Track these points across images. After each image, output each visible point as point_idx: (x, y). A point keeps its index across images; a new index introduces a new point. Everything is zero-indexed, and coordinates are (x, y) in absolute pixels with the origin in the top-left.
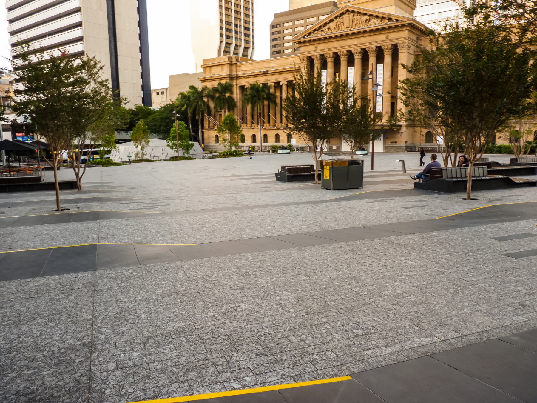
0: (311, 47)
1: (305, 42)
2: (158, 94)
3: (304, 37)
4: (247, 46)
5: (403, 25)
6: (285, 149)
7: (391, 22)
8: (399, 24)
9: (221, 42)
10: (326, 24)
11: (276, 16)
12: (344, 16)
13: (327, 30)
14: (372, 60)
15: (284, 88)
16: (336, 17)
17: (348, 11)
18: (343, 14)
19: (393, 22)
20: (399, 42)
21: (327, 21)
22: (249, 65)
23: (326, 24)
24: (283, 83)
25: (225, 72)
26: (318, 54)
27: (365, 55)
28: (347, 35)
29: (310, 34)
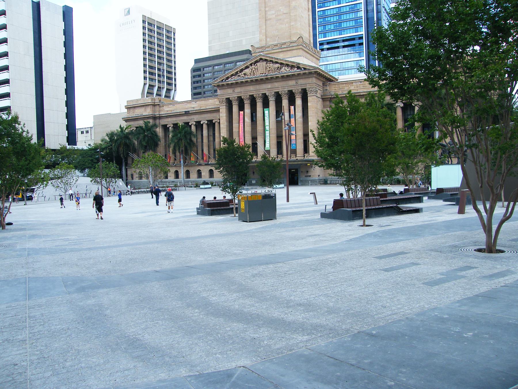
0: (229, 89)
1: (223, 85)
2: (82, 133)
3: (222, 81)
4: (169, 87)
5: (310, 73)
6: (207, 184)
9: (145, 84)
10: (242, 71)
11: (197, 61)
12: (258, 64)
14: (285, 103)
15: (205, 127)
16: (251, 65)
17: (261, 59)
18: (256, 62)
19: (301, 69)
20: (307, 87)
22: (171, 106)
23: (242, 71)
24: (204, 122)
25: (148, 112)
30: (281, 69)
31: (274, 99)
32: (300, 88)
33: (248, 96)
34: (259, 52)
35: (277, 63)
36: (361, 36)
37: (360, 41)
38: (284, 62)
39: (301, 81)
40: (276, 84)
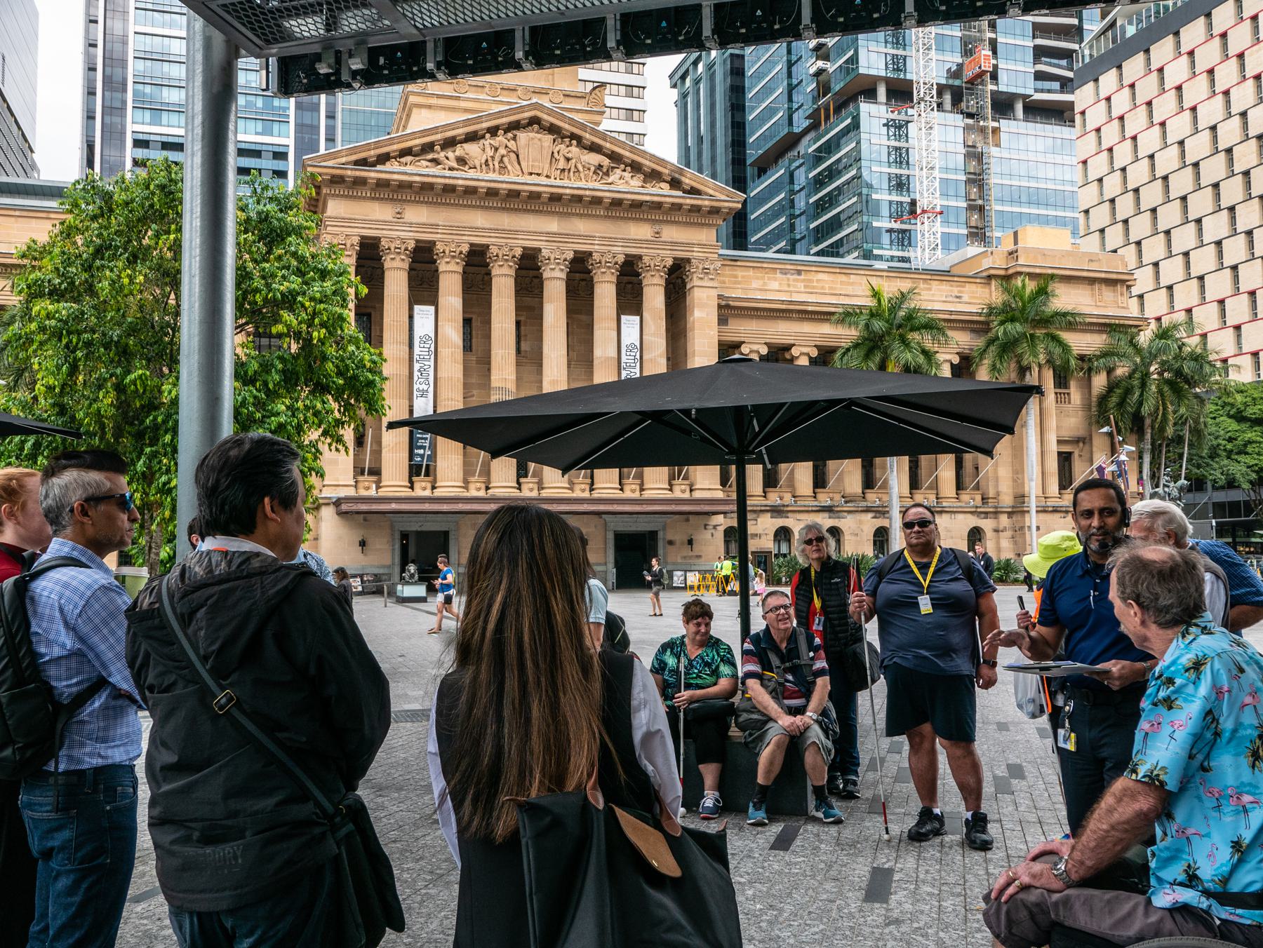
1: (360, 182)
7: (680, 193)
8: (706, 203)
10: (450, 143)
12: (523, 136)
13: (456, 165)
14: (605, 294)
16: (493, 131)
17: (534, 121)
18: (514, 126)
20: (696, 254)
21: (460, 132)
23: (450, 143)
26: (410, 237)
28: (534, 196)
29: (384, 158)
30: (607, 174)
31: (564, 276)
33: (465, 248)
34: (439, 96)
35: (594, 148)
36: (281, 150)
37: (278, 165)
38: (627, 154)
39: (671, 233)
40: (581, 226)
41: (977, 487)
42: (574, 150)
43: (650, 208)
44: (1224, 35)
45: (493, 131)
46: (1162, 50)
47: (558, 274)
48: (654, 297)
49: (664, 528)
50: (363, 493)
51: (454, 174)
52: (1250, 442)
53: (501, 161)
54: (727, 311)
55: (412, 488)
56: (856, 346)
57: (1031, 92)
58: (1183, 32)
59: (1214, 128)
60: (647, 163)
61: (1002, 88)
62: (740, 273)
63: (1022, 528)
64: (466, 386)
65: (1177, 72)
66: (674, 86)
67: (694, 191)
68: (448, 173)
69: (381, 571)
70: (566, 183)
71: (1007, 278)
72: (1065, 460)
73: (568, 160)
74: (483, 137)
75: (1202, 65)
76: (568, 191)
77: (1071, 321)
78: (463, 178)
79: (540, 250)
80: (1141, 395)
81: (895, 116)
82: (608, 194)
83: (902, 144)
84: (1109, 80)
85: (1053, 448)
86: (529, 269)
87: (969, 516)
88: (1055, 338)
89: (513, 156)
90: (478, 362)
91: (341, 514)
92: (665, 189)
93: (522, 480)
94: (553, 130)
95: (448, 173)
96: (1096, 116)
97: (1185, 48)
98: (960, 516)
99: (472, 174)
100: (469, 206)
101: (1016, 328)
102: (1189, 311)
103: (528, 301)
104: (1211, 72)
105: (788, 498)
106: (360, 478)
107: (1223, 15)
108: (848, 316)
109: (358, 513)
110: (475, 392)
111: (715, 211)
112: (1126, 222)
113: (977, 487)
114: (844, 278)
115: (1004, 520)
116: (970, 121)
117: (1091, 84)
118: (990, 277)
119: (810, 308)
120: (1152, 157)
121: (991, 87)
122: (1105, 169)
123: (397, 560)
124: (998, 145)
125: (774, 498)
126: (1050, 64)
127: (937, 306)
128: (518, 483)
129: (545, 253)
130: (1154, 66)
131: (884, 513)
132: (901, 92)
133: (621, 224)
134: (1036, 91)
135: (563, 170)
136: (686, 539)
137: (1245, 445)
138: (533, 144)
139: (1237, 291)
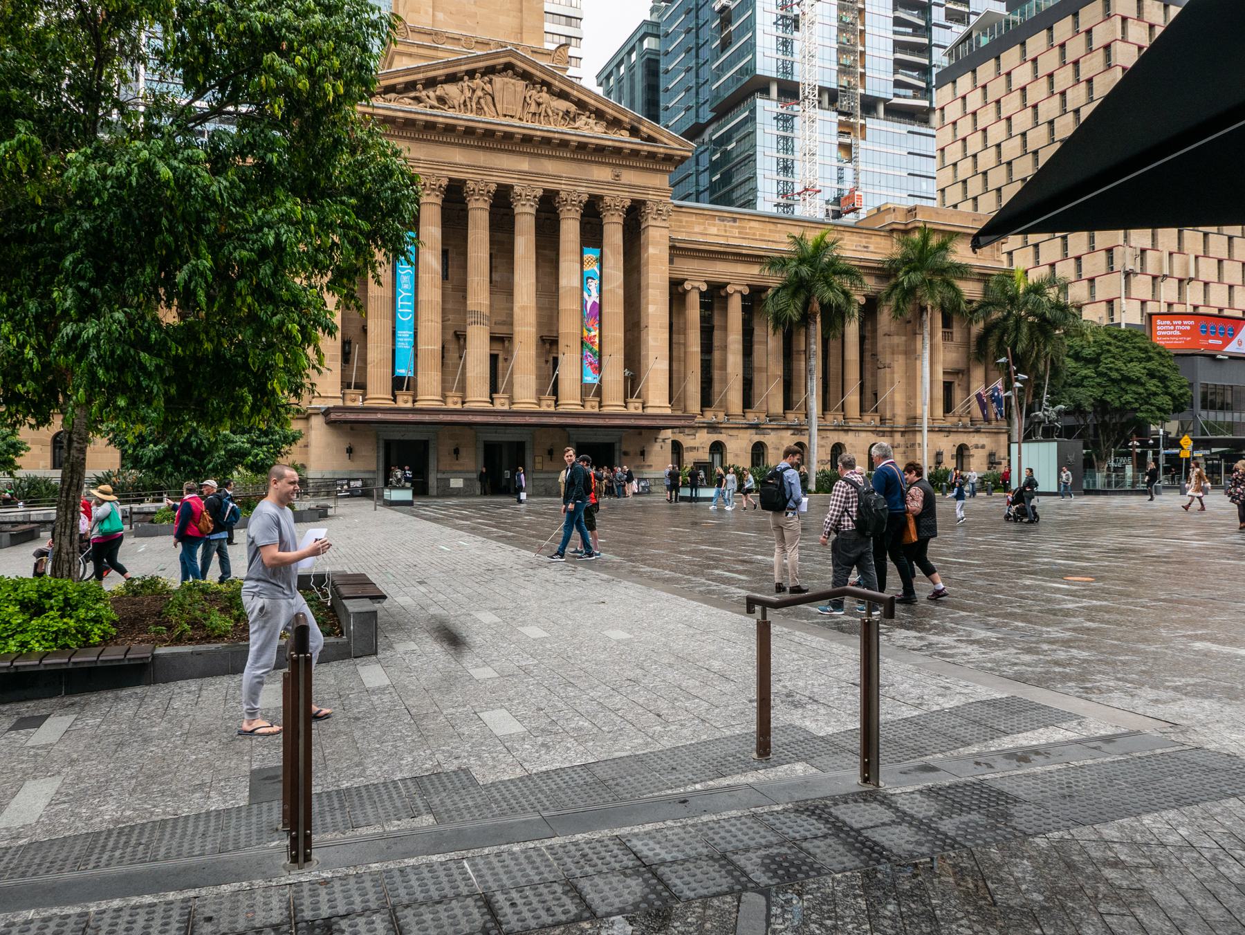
7: (638, 141)
10: (431, 83)
12: (498, 80)
13: (436, 104)
14: (570, 230)
16: (471, 74)
17: (508, 67)
18: (490, 71)
20: (651, 197)
23: (431, 83)
27: (548, 207)
28: (508, 136)
31: (533, 211)
32: (626, 198)
33: (445, 182)
34: (419, 46)
35: (562, 95)
38: (592, 102)
39: (629, 177)
40: (550, 166)
41: (876, 410)
42: (545, 96)
43: (612, 152)
44: (1062, 46)
45: (471, 74)
46: (1011, 57)
47: (528, 209)
48: (614, 234)
49: (620, 441)
50: (349, 404)
51: (435, 111)
52: (1086, 377)
53: (478, 103)
54: (677, 251)
55: (395, 400)
56: (784, 287)
57: (891, 97)
58: (1030, 42)
59: (1051, 123)
60: (610, 111)
61: (869, 93)
62: (685, 218)
63: (913, 445)
64: (444, 310)
65: (1022, 75)
66: (600, 85)
67: (650, 139)
68: (429, 111)
69: (367, 476)
70: (536, 125)
71: (906, 232)
72: (948, 387)
73: (539, 104)
74: (462, 79)
75: (1043, 70)
76: (538, 133)
77: (962, 271)
78: (444, 116)
79: (512, 187)
80: (1016, 336)
81: (783, 111)
82: (574, 138)
83: (788, 134)
84: (965, 82)
85: (940, 377)
86: (502, 202)
87: (870, 434)
88: (950, 285)
89: (489, 97)
90: (454, 289)
91: (331, 423)
92: (624, 136)
93: (494, 396)
94: (525, 76)
95: (429, 111)
96: (953, 112)
97: (1029, 56)
98: (863, 435)
99: (451, 113)
100: (448, 143)
101: (916, 277)
102: (1052, 265)
103: (501, 236)
104: (1051, 76)
105: (721, 416)
106: (348, 391)
107: (1090, 15)
108: (776, 263)
109: (346, 422)
110: (450, 317)
111: (668, 158)
112: (975, 199)
113: (876, 410)
114: (772, 227)
115: (898, 437)
116: (843, 118)
117: (950, 85)
118: (892, 231)
119: (744, 252)
120: (998, 146)
121: (861, 91)
122: (959, 156)
123: (381, 466)
124: (864, 139)
125: (710, 416)
126: (906, 75)
127: (849, 254)
128: (491, 398)
129: (517, 189)
130: (1004, 70)
131: (801, 430)
132: (789, 91)
133: (585, 166)
134: (896, 95)
135: (534, 114)
136: (638, 450)
137: (1082, 380)
138: (508, 89)
139: (1065, 256)
